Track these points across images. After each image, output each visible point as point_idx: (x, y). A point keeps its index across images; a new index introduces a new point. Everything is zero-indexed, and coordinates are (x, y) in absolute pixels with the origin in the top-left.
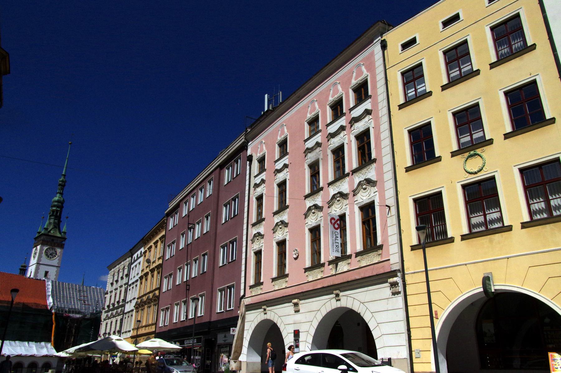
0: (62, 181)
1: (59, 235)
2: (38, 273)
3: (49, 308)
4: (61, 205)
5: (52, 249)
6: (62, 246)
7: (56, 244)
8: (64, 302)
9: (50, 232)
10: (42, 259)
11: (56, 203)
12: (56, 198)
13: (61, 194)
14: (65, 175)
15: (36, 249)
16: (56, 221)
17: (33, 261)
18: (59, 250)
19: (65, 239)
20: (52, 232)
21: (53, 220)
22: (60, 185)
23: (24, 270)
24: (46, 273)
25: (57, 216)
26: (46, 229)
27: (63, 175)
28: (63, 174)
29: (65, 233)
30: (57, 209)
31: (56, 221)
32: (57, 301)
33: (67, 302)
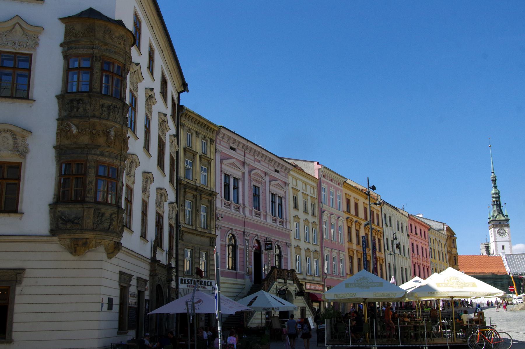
0: (493, 177)
1: (503, 218)
2: (497, 248)
3: (508, 274)
4: (497, 196)
5: (502, 229)
6: (508, 226)
7: (503, 226)
8: (517, 268)
9: (496, 218)
10: (497, 238)
11: (494, 195)
12: (493, 192)
13: (496, 187)
14: (493, 172)
15: (491, 231)
16: (498, 208)
17: (492, 239)
18: (506, 229)
19: (508, 220)
20: (497, 217)
21: (496, 208)
22: (492, 181)
23: (487, 248)
24: (503, 247)
25: (498, 204)
26: (493, 216)
27: (492, 172)
28: (492, 171)
29: (507, 216)
30: (496, 199)
31: (498, 208)
32: (512, 268)
33: (519, 268)
